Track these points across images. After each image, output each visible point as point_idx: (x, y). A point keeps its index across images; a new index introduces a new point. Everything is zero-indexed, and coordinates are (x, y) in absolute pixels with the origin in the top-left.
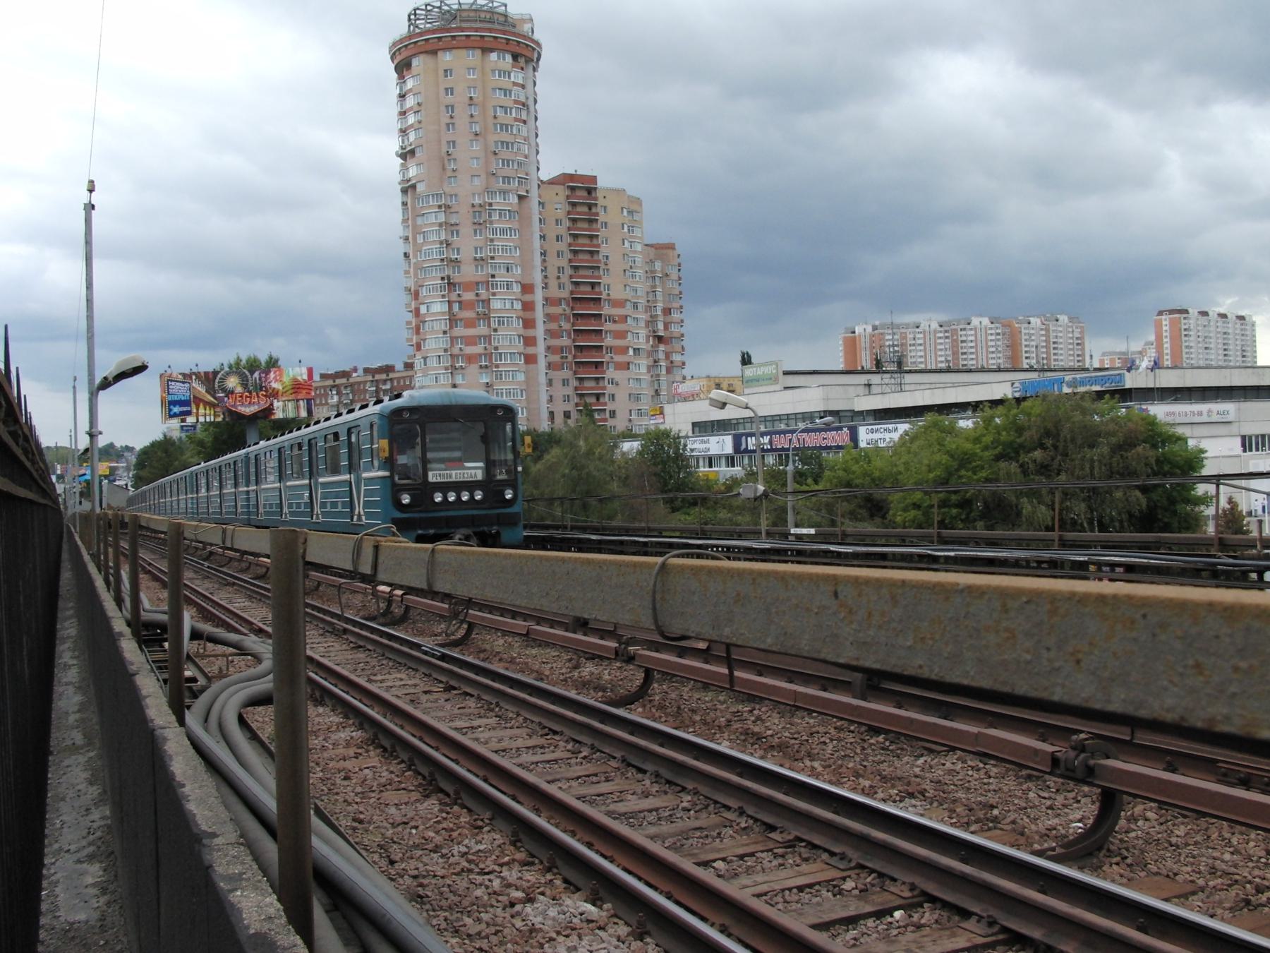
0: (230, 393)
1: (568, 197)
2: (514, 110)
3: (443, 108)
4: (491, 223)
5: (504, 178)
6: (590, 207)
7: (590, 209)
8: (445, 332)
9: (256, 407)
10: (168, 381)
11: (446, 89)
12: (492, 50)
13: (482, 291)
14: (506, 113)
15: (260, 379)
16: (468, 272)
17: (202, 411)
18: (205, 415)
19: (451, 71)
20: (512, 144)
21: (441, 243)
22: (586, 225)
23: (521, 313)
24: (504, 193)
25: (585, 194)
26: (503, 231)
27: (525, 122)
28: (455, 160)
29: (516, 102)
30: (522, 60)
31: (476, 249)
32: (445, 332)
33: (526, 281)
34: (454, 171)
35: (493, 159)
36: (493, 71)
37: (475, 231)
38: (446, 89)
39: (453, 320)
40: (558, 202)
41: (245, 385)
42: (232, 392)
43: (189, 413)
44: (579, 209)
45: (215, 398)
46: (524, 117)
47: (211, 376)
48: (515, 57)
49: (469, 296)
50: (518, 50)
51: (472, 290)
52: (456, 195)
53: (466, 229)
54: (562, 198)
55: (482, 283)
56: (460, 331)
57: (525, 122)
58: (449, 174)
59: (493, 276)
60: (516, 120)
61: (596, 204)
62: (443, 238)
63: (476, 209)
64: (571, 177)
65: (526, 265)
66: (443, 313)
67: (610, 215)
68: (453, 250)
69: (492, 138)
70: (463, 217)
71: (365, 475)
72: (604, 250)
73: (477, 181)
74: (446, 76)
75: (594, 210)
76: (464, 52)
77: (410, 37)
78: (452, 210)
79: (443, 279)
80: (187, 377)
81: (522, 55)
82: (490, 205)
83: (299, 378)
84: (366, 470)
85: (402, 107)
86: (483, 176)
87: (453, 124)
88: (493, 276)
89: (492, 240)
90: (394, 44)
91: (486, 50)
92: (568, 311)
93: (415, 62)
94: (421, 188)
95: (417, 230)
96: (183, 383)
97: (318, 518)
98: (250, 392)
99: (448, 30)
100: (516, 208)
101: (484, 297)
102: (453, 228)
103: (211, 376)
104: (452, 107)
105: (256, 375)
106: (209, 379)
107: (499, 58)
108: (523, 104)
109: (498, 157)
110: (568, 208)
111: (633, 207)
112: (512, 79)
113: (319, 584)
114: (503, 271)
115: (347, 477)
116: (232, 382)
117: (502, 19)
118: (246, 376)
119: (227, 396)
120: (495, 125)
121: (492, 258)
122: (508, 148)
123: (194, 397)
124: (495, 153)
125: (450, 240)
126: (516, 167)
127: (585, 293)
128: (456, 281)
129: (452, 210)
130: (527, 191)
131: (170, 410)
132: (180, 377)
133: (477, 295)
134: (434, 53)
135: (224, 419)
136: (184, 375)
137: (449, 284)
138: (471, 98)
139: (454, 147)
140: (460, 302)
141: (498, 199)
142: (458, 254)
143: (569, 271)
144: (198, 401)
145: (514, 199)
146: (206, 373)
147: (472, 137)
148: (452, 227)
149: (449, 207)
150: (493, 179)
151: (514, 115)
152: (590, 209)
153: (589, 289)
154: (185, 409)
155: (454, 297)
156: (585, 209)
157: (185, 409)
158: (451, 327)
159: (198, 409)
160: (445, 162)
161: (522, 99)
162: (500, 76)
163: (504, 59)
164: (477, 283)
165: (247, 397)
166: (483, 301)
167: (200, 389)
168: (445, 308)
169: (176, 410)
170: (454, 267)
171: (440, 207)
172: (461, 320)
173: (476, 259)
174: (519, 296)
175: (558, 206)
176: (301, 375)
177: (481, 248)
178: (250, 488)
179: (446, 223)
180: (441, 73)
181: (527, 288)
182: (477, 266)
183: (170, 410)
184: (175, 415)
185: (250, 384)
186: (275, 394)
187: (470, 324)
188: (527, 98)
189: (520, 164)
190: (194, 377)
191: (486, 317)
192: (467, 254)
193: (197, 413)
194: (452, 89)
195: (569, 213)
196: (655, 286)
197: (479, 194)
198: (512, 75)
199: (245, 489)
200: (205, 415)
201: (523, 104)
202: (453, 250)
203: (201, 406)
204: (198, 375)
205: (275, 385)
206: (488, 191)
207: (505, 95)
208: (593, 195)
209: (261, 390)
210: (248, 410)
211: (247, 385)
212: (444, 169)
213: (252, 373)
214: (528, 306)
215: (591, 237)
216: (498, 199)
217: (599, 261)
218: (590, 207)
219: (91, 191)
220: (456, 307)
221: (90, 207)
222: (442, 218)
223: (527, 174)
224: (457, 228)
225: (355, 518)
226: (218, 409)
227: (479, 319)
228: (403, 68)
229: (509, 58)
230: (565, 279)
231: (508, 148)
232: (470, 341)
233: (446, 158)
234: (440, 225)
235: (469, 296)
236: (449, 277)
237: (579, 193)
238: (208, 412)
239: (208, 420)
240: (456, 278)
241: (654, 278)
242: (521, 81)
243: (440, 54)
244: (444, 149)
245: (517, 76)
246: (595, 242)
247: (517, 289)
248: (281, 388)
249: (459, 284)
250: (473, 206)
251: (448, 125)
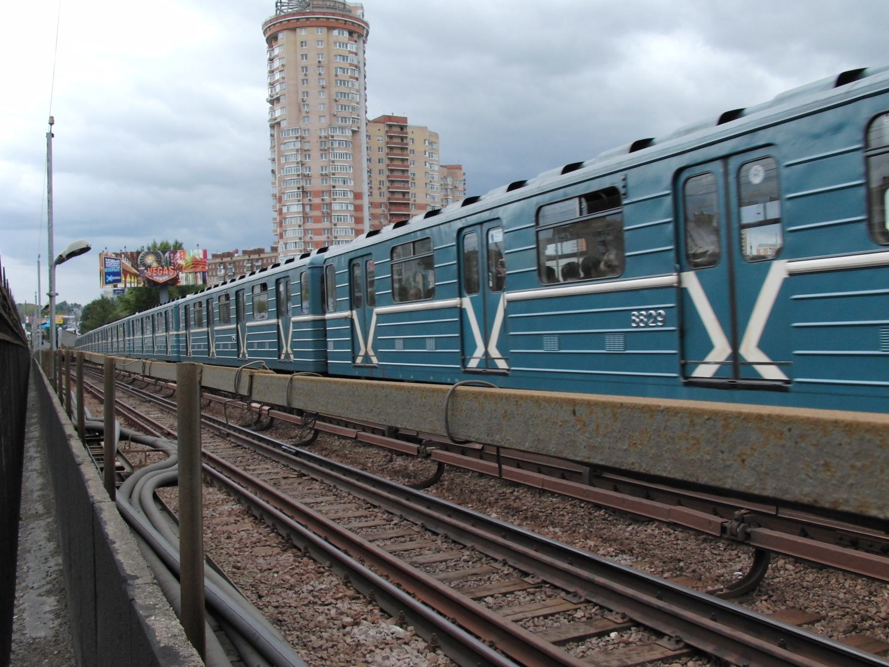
0: (148, 267)
1: (387, 132)
2: (349, 71)
3: (300, 69)
4: (333, 149)
5: (342, 118)
6: (402, 139)
7: (402, 140)
8: (300, 226)
9: (167, 277)
10: (105, 258)
11: (302, 55)
12: (334, 28)
14: (344, 73)
15: (170, 257)
16: (316, 184)
17: (128, 279)
18: (131, 283)
19: (306, 42)
20: (348, 94)
21: (298, 163)
22: (399, 152)
23: (353, 213)
24: (342, 128)
25: (399, 130)
26: (341, 155)
27: (357, 79)
28: (308, 105)
29: (351, 65)
30: (355, 36)
31: (322, 168)
32: (300, 226)
33: (358, 191)
34: (307, 113)
35: (334, 104)
36: (335, 43)
37: (322, 155)
38: (302, 55)
39: (305, 218)
40: (380, 136)
41: (159, 262)
42: (150, 267)
43: (119, 281)
44: (395, 140)
45: (138, 271)
46: (357, 76)
47: (135, 255)
48: (351, 33)
49: (317, 201)
50: (352, 28)
51: (319, 196)
52: (308, 130)
53: (315, 154)
54: (383, 132)
55: (327, 191)
56: (310, 225)
57: (357, 79)
58: (304, 114)
59: (334, 187)
60: (351, 77)
61: (407, 137)
62: (299, 160)
63: (323, 139)
64: (389, 118)
65: (357, 178)
66: (298, 213)
67: (416, 145)
68: (306, 168)
69: (334, 90)
70: (314, 146)
72: (412, 169)
73: (323, 120)
74: (302, 46)
75: (405, 141)
76: (315, 29)
77: (277, 18)
78: (306, 140)
79: (299, 188)
80: (118, 255)
81: (356, 32)
82: (332, 137)
83: (197, 257)
85: (271, 68)
86: (328, 117)
87: (307, 80)
88: (334, 187)
89: (333, 162)
90: (266, 23)
91: (330, 28)
92: (386, 212)
93: (281, 36)
94: (284, 124)
95: (281, 154)
96: (116, 259)
98: (163, 267)
99: (304, 14)
100: (350, 139)
101: (327, 201)
102: (307, 153)
103: (135, 255)
104: (306, 68)
105: (167, 254)
106: (134, 257)
107: (339, 34)
108: (356, 67)
109: (338, 103)
110: (387, 139)
111: (432, 139)
112: (349, 49)
113: (210, 401)
114: (341, 184)
116: (150, 260)
117: (341, 6)
118: (160, 256)
119: (146, 269)
120: (336, 80)
121: (334, 174)
122: (345, 97)
123: (123, 270)
124: (336, 101)
125: (304, 161)
126: (350, 111)
127: (398, 198)
128: (308, 190)
129: (306, 140)
130: (358, 128)
131: (106, 279)
132: (114, 255)
133: (323, 200)
134: (294, 29)
135: (144, 285)
136: (116, 254)
137: (303, 192)
138: (319, 62)
139: (307, 96)
140: (310, 205)
141: (338, 133)
142: (309, 171)
143: (387, 184)
144: (126, 272)
145: (349, 133)
146: (132, 253)
147: (320, 89)
148: (305, 152)
149: (303, 138)
150: (334, 119)
151: (349, 74)
152: (402, 140)
153: (401, 196)
154: (117, 278)
155: (306, 201)
156: (399, 141)
157: (117, 278)
158: (304, 223)
159: (125, 278)
160: (301, 106)
161: (355, 63)
162: (340, 46)
163: (343, 34)
164: (323, 192)
165: (160, 270)
166: (327, 204)
167: (128, 264)
168: (300, 209)
169: (110, 278)
170: (306, 180)
171: (297, 138)
172: (311, 217)
173: (322, 175)
174: (352, 201)
175: (380, 138)
176: (199, 255)
177: (326, 167)
179: (301, 149)
180: (299, 43)
181: (358, 196)
182: (322, 180)
183: (106, 279)
184: (110, 282)
185: (163, 261)
186: (180, 268)
187: (317, 220)
188: (359, 62)
189: (353, 108)
190: (123, 256)
191: (329, 215)
192: (315, 171)
193: (125, 281)
194: (306, 55)
195: (387, 143)
196: (447, 195)
197: (325, 129)
198: (349, 46)
200: (131, 283)
201: (356, 67)
202: (306, 168)
203: (128, 276)
204: (126, 254)
205: (180, 262)
206: (331, 127)
207: (344, 60)
208: (405, 130)
209: (171, 265)
210: (161, 279)
211: (160, 261)
212: (300, 111)
213: (164, 253)
214: (358, 208)
215: (403, 160)
216: (338, 133)
217: (408, 177)
219: (51, 124)
220: (308, 208)
221: (51, 135)
222: (298, 145)
223: (358, 116)
224: (310, 153)
226: (140, 278)
227: (324, 217)
228: (272, 40)
229: (346, 34)
230: (384, 189)
231: (345, 97)
232: (318, 232)
233: (302, 103)
234: (297, 150)
235: (317, 201)
236: (303, 187)
237: (394, 129)
238: (133, 280)
239: (133, 286)
240: (308, 187)
241: (446, 189)
242: (354, 50)
243: (298, 30)
244: (301, 97)
245: (352, 47)
246: (405, 163)
247: (350, 196)
248: (184, 264)
249: (310, 192)
250: (320, 137)
251: (303, 80)
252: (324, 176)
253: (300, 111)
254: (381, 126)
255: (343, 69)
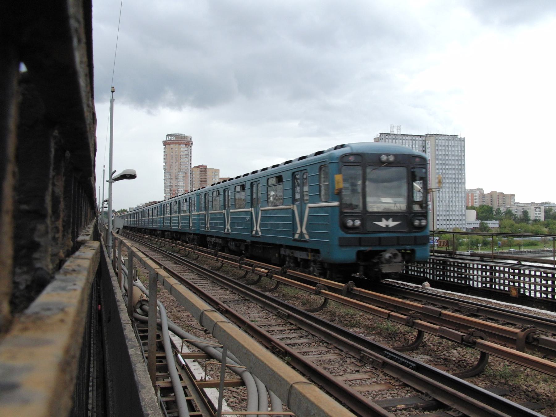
6: (205, 172)
13: (177, 192)
16: (174, 188)
22: (204, 176)
25: (204, 169)
30: (187, 146)
40: (197, 173)
46: (187, 157)
48: (186, 145)
50: (186, 144)
54: (199, 170)
64: (201, 166)
65: (186, 187)
70: (173, 177)
71: (210, 212)
77: (165, 141)
84: (211, 210)
93: (167, 146)
97: (191, 228)
113: (180, 249)
114: (181, 188)
115: (204, 212)
117: (184, 137)
134: (170, 144)
155: (171, 193)
156: (204, 173)
164: (176, 190)
168: (170, 195)
178: (162, 216)
189: (186, 166)
199: (160, 217)
212: (170, 167)
218: (205, 172)
220: (171, 194)
222: (170, 177)
225: (206, 228)
229: (184, 146)
235: (174, 193)
237: (203, 169)
240: (172, 189)
245: (186, 149)
252: (176, 186)
253: (170, 167)
254: (198, 168)
255: (183, 156)
